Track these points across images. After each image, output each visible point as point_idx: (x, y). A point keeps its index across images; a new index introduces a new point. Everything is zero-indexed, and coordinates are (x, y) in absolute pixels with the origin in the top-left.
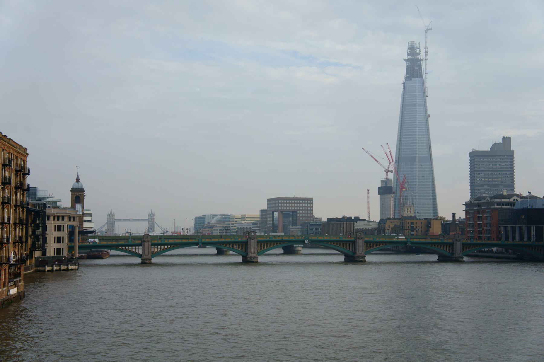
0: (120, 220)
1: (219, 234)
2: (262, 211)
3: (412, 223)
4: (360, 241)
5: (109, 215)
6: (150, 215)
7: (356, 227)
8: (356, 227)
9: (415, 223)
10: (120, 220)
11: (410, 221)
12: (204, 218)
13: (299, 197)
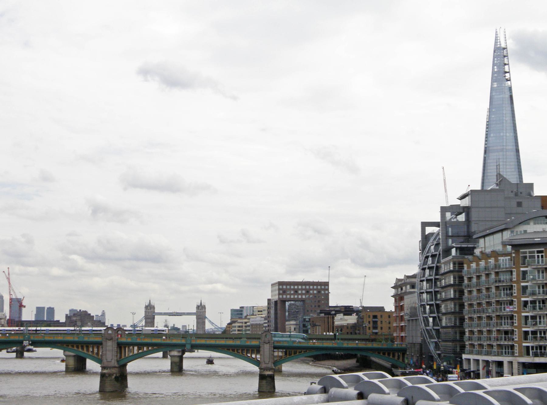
0: (160, 314)
1: (237, 332)
2: (269, 300)
3: (375, 317)
4: (109, 343)
5: (146, 307)
6: (198, 307)
7: (336, 323)
8: (336, 323)
9: (379, 317)
10: (160, 314)
11: (372, 314)
12: (242, 311)
13: (311, 280)
